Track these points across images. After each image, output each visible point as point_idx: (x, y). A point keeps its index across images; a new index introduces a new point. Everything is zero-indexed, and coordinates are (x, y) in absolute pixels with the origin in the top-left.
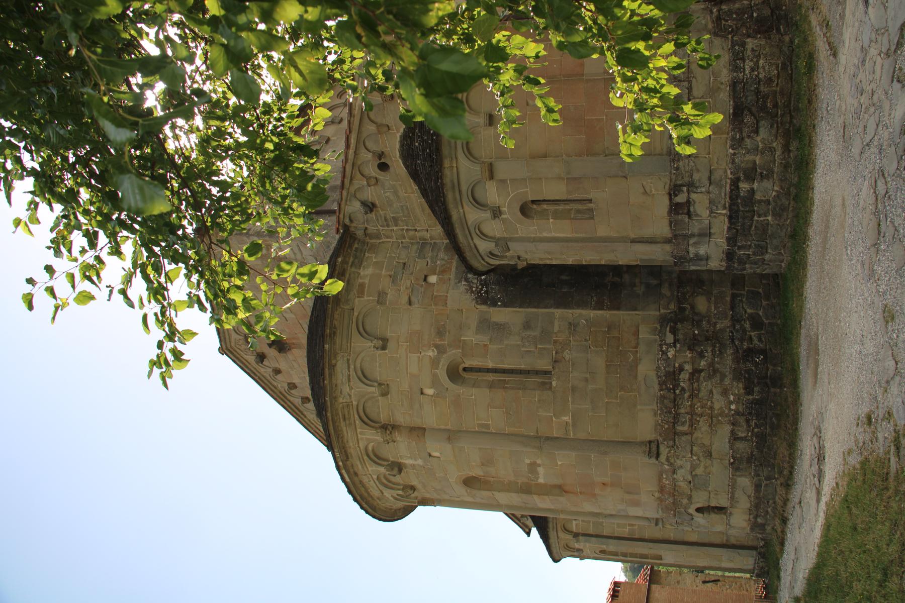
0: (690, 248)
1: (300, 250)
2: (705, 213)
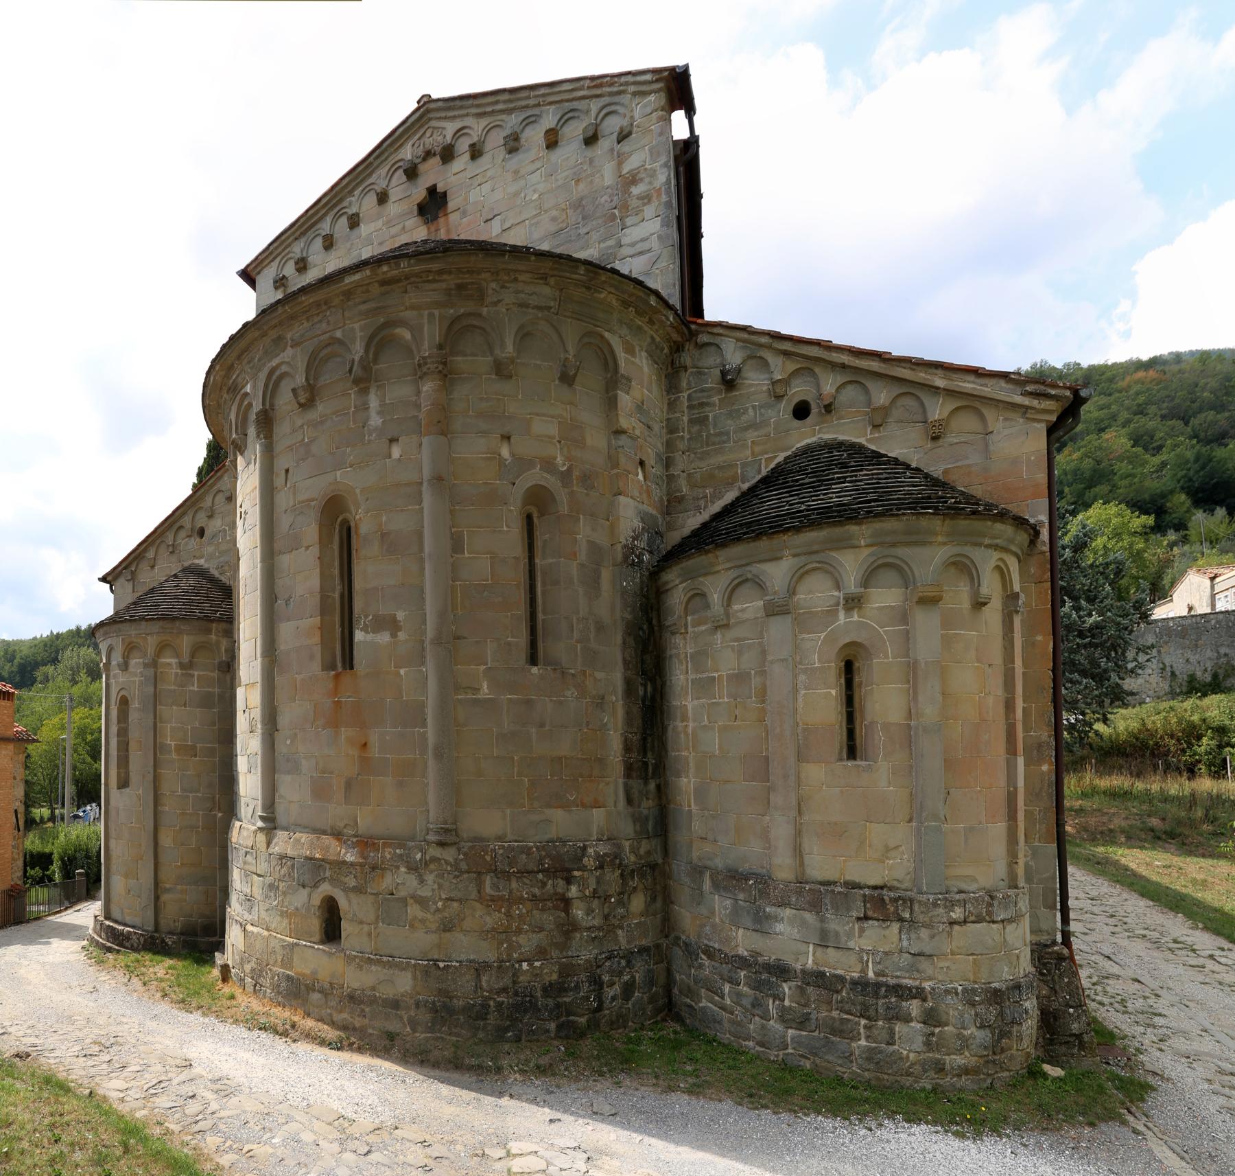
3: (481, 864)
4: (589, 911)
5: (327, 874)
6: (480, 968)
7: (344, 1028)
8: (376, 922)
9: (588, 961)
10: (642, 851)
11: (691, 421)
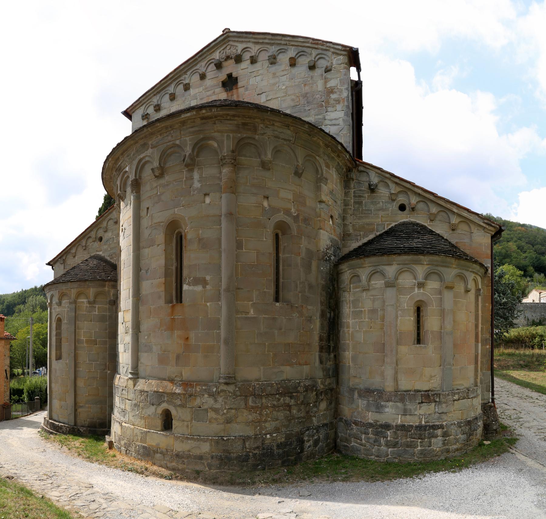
0: (391, 403)
1: (335, 125)
2: (422, 412)
3: (248, 393)
4: (299, 410)
5: (166, 399)
6: (245, 439)
7: (173, 469)
8: (191, 420)
9: (297, 432)
10: (326, 383)
11: (354, 202)
